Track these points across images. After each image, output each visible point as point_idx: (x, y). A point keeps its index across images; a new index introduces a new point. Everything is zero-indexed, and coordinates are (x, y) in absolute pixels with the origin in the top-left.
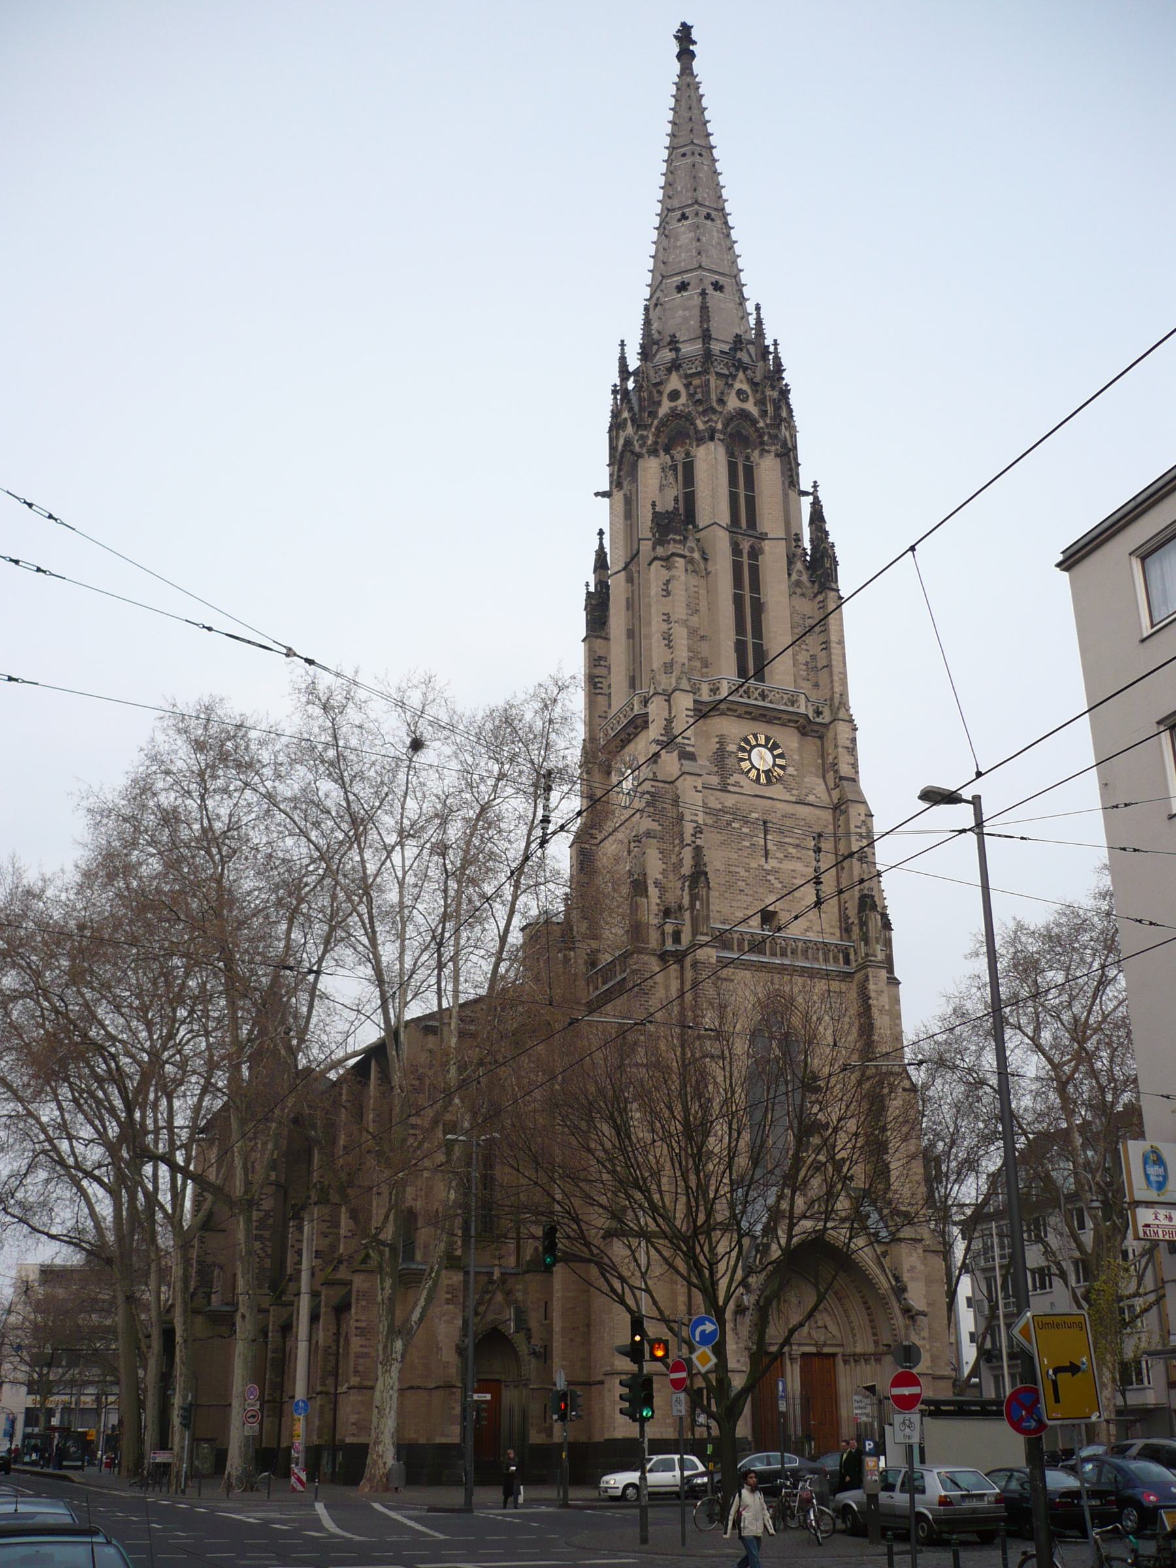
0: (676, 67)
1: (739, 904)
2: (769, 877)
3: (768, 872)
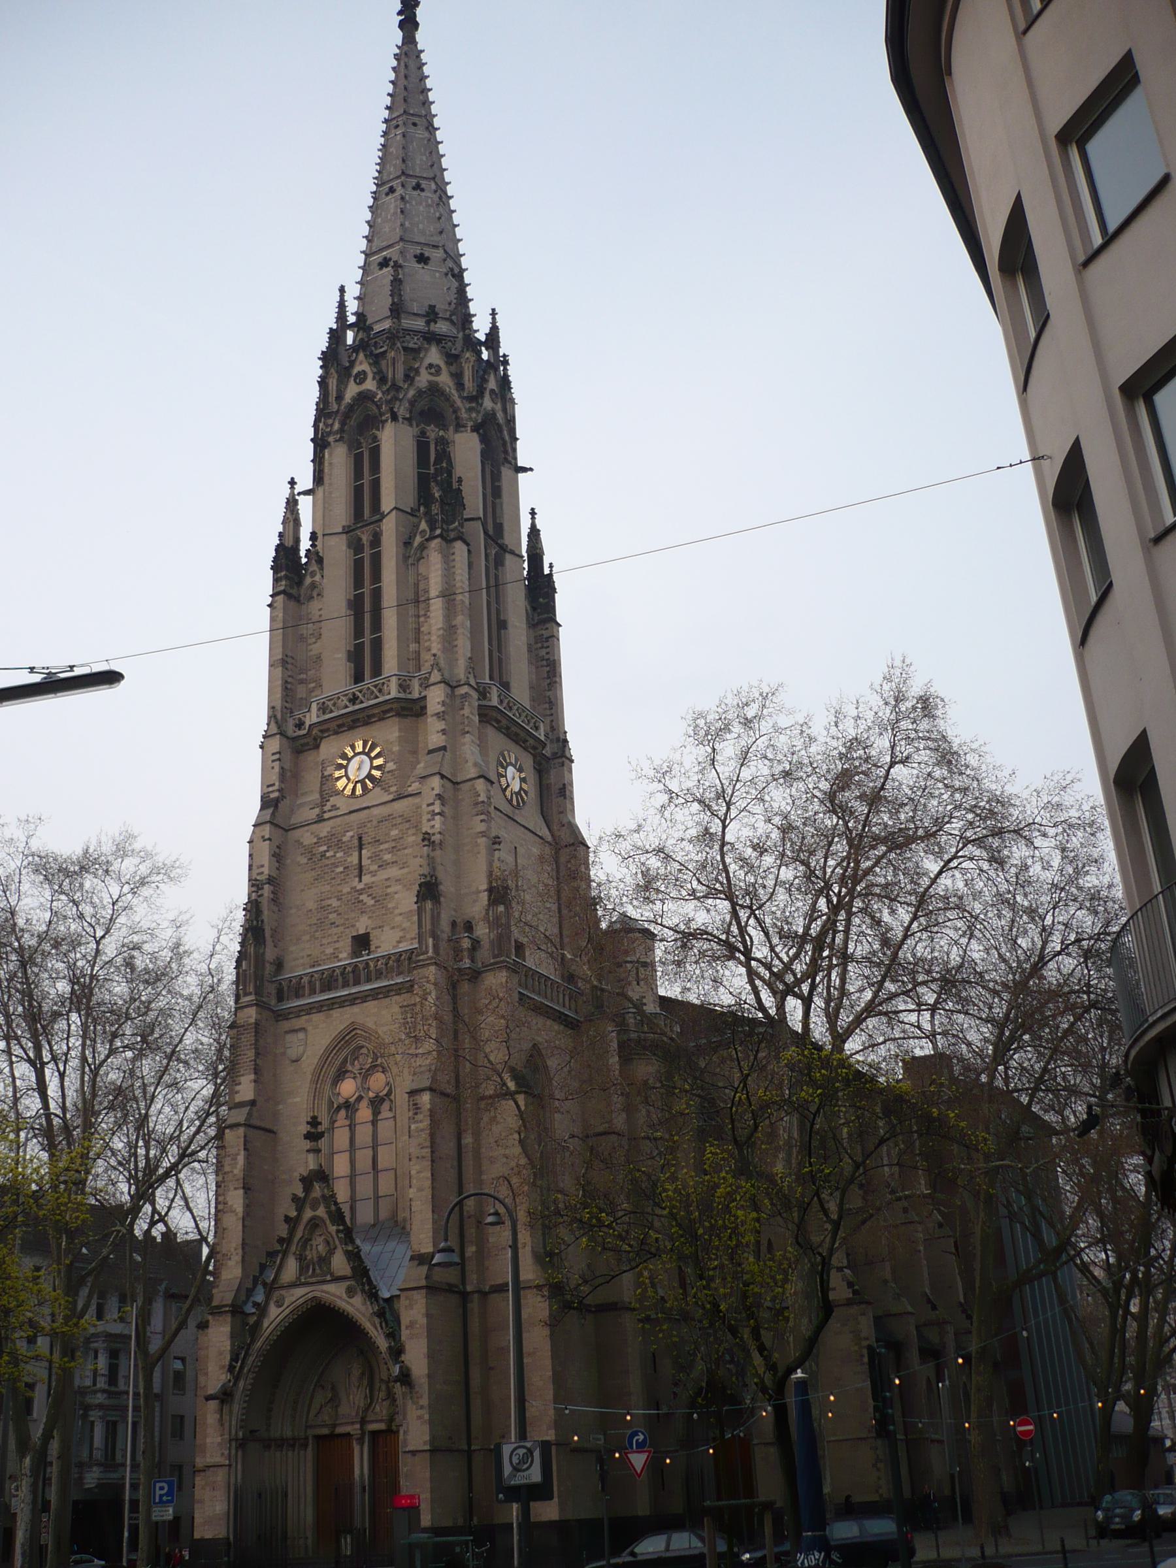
0: (398, 37)
2: (361, 897)
3: (361, 892)
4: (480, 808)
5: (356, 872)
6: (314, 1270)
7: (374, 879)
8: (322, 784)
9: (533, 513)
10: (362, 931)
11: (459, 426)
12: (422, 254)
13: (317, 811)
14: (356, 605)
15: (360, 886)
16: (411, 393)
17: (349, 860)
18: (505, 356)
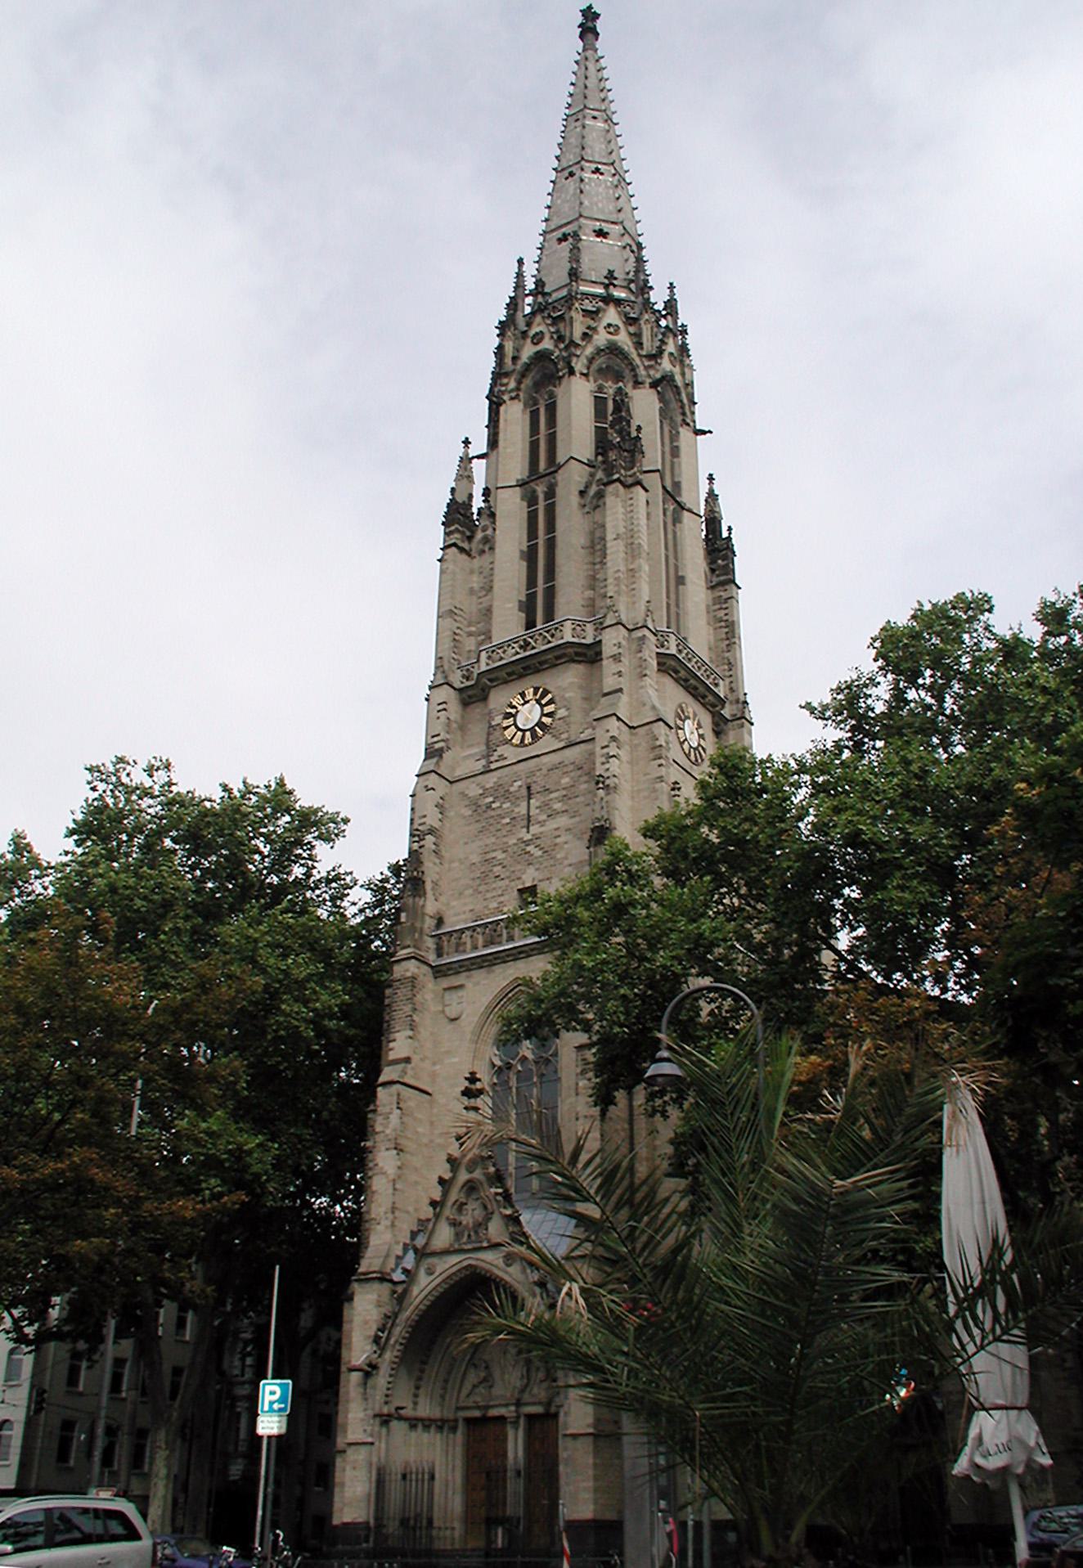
1: (494, 894)
2: (528, 849)
3: (527, 843)
4: (657, 752)
5: (525, 822)
6: (469, 1236)
7: (542, 829)
8: (489, 734)
9: (711, 478)
10: (528, 884)
11: (637, 384)
12: (601, 230)
13: (483, 762)
14: (530, 556)
15: (529, 837)
16: (589, 350)
17: (517, 810)
18: (683, 325)
